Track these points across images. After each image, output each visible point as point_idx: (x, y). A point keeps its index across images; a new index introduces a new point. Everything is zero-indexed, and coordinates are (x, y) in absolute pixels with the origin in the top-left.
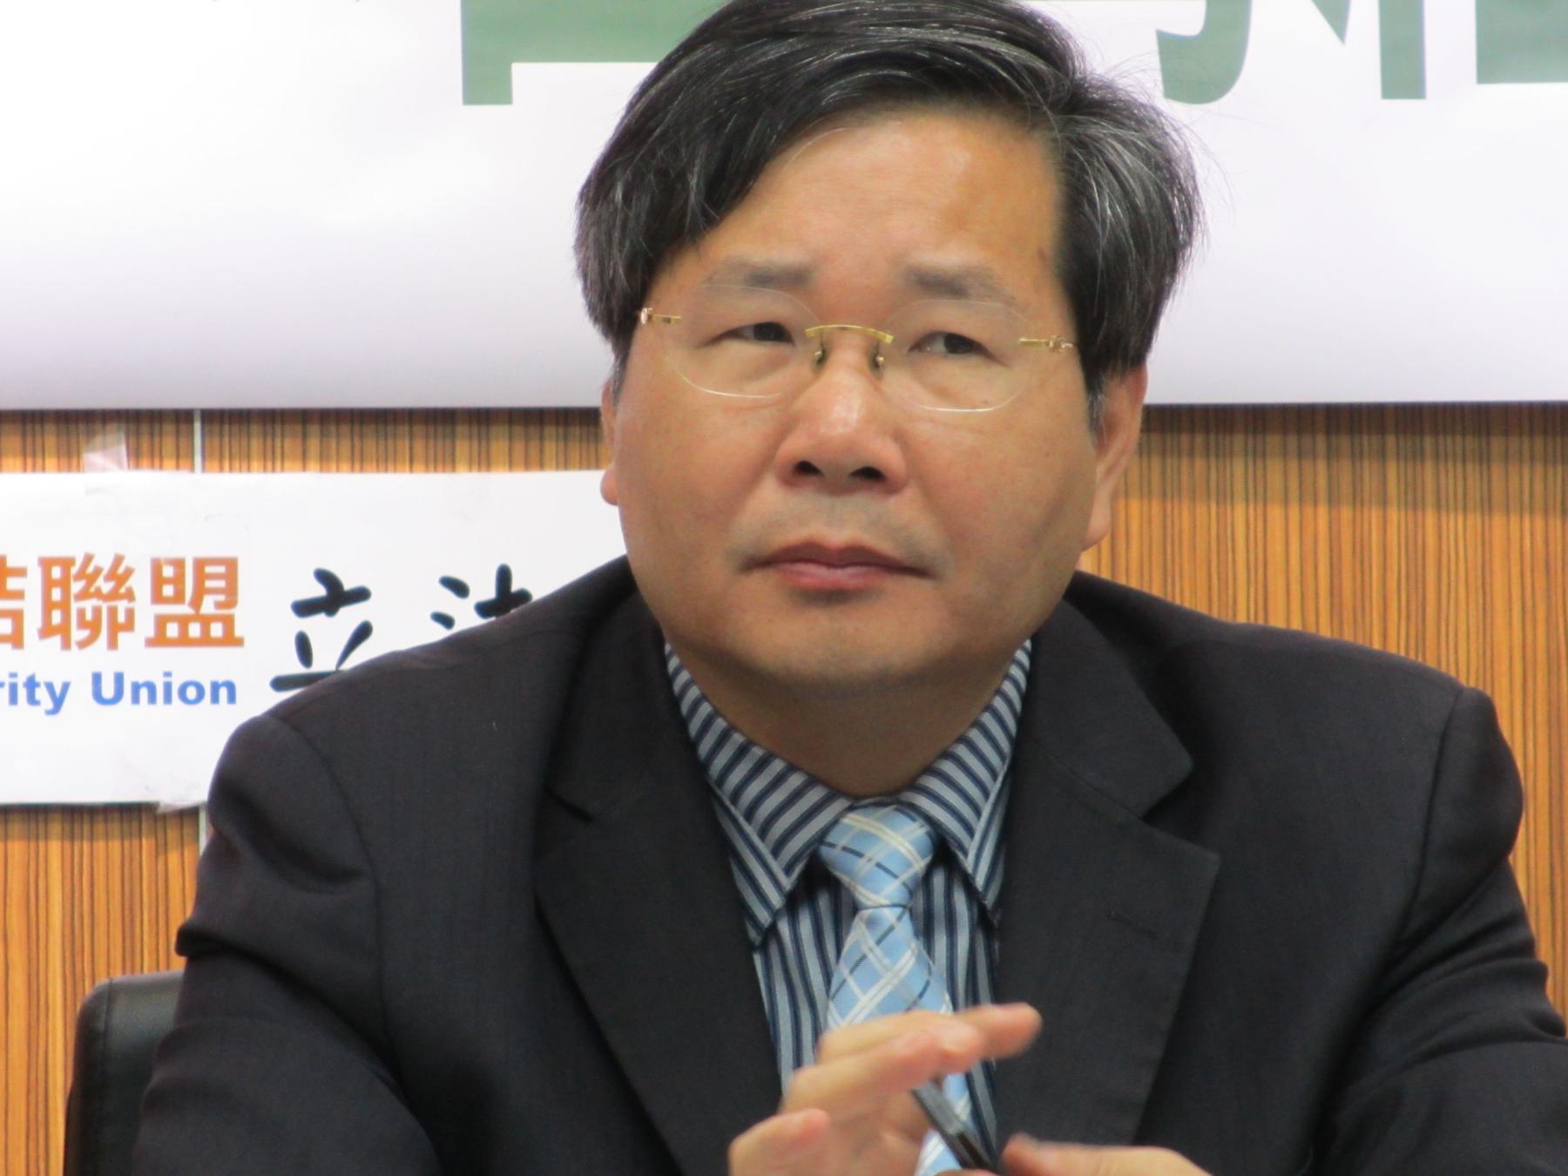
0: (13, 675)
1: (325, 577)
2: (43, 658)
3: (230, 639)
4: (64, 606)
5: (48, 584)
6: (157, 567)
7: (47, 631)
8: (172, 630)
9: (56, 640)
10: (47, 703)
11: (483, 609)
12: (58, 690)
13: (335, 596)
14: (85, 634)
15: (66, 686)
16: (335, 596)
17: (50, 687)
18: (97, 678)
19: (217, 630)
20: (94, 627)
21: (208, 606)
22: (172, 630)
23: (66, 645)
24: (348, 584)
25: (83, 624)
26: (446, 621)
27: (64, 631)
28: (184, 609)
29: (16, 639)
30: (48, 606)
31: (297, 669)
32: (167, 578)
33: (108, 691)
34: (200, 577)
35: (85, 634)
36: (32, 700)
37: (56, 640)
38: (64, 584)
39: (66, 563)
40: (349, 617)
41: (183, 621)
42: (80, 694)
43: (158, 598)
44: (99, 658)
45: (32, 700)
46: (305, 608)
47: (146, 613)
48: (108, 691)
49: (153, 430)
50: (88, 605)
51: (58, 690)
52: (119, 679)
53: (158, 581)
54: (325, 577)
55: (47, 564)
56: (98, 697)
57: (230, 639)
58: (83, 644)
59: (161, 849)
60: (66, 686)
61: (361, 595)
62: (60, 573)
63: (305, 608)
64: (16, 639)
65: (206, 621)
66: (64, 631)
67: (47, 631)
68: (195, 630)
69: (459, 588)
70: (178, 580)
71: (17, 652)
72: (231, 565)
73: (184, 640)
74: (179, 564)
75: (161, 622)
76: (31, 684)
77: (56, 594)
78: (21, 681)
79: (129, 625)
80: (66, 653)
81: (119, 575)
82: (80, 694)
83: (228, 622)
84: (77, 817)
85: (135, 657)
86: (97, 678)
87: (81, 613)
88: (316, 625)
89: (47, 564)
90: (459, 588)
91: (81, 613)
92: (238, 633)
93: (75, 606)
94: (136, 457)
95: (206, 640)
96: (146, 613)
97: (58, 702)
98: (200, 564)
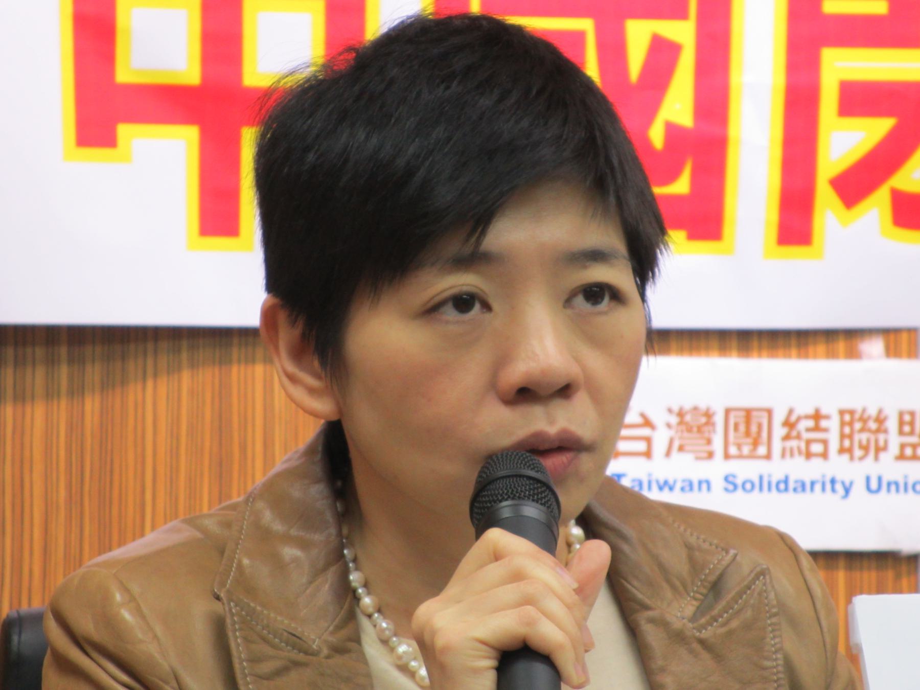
2: (839, 466)
4: (851, 437)
5: (843, 424)
6: (901, 415)
7: (842, 450)
22: (909, 451)
29: (825, 455)
30: (843, 436)
33: (874, 485)
38: (851, 424)
39: (852, 412)
43: (901, 432)
44: (869, 467)
47: (894, 441)
48: (874, 485)
53: (901, 423)
55: (842, 413)
62: (848, 417)
64: (825, 455)
67: (842, 450)
75: (903, 447)
79: (885, 448)
81: (880, 420)
85: (888, 467)
89: (842, 413)
97: (847, 491)
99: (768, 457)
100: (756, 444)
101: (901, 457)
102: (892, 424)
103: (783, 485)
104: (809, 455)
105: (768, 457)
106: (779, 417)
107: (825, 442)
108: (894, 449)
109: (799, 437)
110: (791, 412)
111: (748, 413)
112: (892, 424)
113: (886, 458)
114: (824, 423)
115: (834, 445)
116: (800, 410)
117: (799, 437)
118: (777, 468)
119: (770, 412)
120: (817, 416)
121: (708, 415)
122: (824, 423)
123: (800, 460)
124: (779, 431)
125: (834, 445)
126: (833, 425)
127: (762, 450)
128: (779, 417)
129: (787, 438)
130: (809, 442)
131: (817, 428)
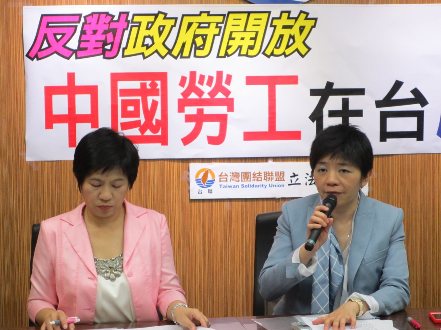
1: (294, 173)
2: (264, 182)
3: (284, 180)
4: (266, 177)
5: (264, 174)
6: (276, 172)
7: (264, 179)
8: (278, 179)
11: (310, 177)
13: (295, 175)
16: (295, 175)
19: (282, 179)
21: (281, 177)
22: (278, 179)
24: (296, 174)
26: (306, 178)
27: (266, 179)
28: (279, 177)
29: (261, 180)
30: (265, 177)
31: (290, 183)
32: (277, 174)
33: (271, 186)
34: (280, 173)
38: (266, 174)
39: (266, 172)
40: (296, 178)
41: (279, 178)
42: (268, 186)
43: (276, 176)
44: (270, 182)
46: (291, 177)
47: (275, 177)
48: (271, 186)
49: (275, 159)
50: (269, 177)
53: (276, 174)
54: (294, 173)
55: (264, 172)
57: (284, 180)
59: (276, 202)
61: (297, 175)
62: (266, 173)
63: (291, 177)
64: (261, 180)
65: (281, 178)
66: (266, 179)
67: (264, 179)
68: (280, 179)
69: (308, 174)
70: (278, 174)
72: (284, 172)
73: (279, 180)
74: (278, 172)
75: (276, 178)
76: (263, 185)
79: (273, 179)
81: (272, 174)
83: (283, 178)
84: (267, 199)
85: (274, 182)
88: (293, 179)
89: (264, 172)
90: (308, 174)
92: (285, 179)
94: (274, 161)
95: (281, 180)
96: (275, 177)
97: (266, 187)
98: (280, 172)
99: (250, 181)
100: (248, 179)
101: (276, 180)
102: (274, 174)
103: (253, 186)
104: (258, 180)
105: (250, 181)
106: (252, 174)
107: (261, 178)
108: (275, 179)
109: (256, 177)
110: (254, 172)
111: (246, 173)
112: (274, 174)
113: (273, 181)
114: (261, 174)
115: (263, 178)
116: (256, 172)
117: (256, 177)
118: (252, 183)
119: (250, 173)
120: (260, 173)
122: (261, 174)
123: (256, 181)
124: (252, 176)
125: (263, 178)
126: (263, 175)
127: (249, 180)
128: (252, 174)
129: (254, 177)
130: (258, 178)
131: (259, 175)
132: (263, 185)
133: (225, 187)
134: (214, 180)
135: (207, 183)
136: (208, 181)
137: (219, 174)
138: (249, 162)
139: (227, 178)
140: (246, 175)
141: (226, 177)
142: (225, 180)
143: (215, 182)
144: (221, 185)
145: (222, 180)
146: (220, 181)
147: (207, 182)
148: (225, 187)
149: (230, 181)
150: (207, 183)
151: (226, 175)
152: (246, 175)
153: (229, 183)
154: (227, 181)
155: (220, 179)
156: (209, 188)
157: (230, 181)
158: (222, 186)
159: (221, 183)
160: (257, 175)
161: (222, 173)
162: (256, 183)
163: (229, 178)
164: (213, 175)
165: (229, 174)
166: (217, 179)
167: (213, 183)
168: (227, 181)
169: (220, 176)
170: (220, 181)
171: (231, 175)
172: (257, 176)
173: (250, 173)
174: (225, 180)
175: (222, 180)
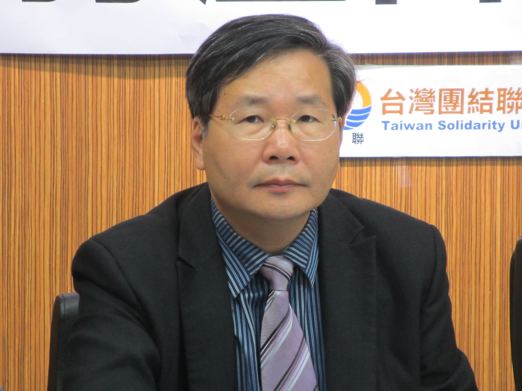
0: (489, 121)
4: (504, 102)
5: (500, 95)
9: (502, 111)
10: (499, 129)
12: (502, 125)
14: (509, 109)
15: (504, 124)
17: (499, 124)
18: (512, 122)
20: (512, 107)
23: (504, 113)
25: (509, 107)
27: (503, 108)
29: (490, 111)
30: (500, 102)
35: (509, 109)
36: (494, 128)
37: (502, 111)
45: (494, 128)
51: (502, 125)
52: (518, 122)
56: (512, 127)
58: (509, 112)
60: (504, 124)
64: (490, 111)
66: (503, 108)
71: (491, 115)
76: (494, 123)
77: (502, 98)
78: (491, 122)
80: (504, 115)
82: (507, 127)
86: (512, 122)
87: (508, 103)
91: (508, 103)
93: (507, 102)
107: (491, 105)
109: (477, 102)
110: (473, 90)
111: (452, 91)
114: (490, 96)
115: (495, 106)
116: (478, 90)
117: (477, 102)
119: (462, 90)
121: (431, 92)
122: (490, 96)
124: (467, 100)
125: (495, 106)
128: (467, 93)
129: (471, 103)
130: (482, 105)
131: (486, 98)
132: (494, 123)
133: (396, 127)
134: (369, 109)
135: (350, 117)
136: (354, 112)
137: (383, 95)
138: (459, 64)
139: (401, 105)
140: (451, 96)
141: (400, 101)
142: (397, 108)
143: (371, 113)
144: (386, 123)
145: (388, 108)
146: (384, 112)
147: (349, 113)
148: (396, 127)
149: (411, 112)
150: (350, 117)
151: (401, 97)
152: (451, 96)
153: (407, 118)
154: (401, 112)
155: (384, 105)
156: (356, 130)
157: (411, 112)
158: (389, 126)
159: (387, 117)
160: (479, 96)
161: (390, 91)
162: (477, 118)
163: (407, 105)
164: (367, 97)
165: (406, 94)
166: (376, 105)
167: (365, 117)
168: (401, 112)
169: (385, 98)
170: (384, 112)
171: (414, 95)
172: (480, 100)
173: (462, 90)
174: (397, 108)
175: (388, 108)
